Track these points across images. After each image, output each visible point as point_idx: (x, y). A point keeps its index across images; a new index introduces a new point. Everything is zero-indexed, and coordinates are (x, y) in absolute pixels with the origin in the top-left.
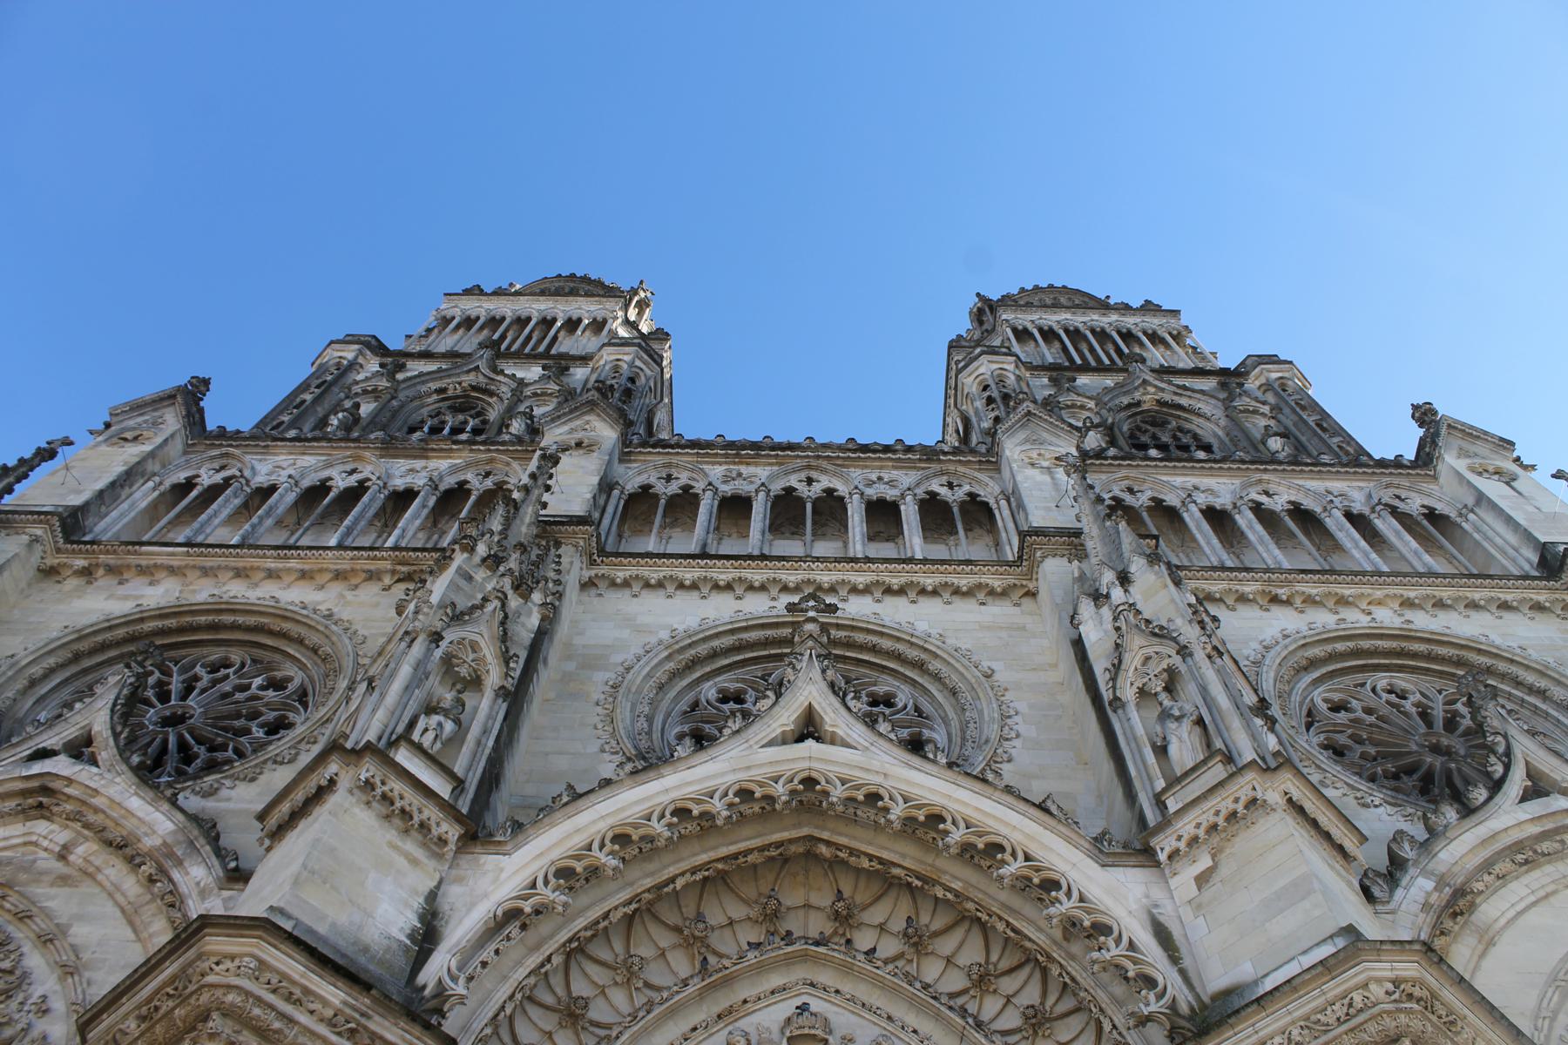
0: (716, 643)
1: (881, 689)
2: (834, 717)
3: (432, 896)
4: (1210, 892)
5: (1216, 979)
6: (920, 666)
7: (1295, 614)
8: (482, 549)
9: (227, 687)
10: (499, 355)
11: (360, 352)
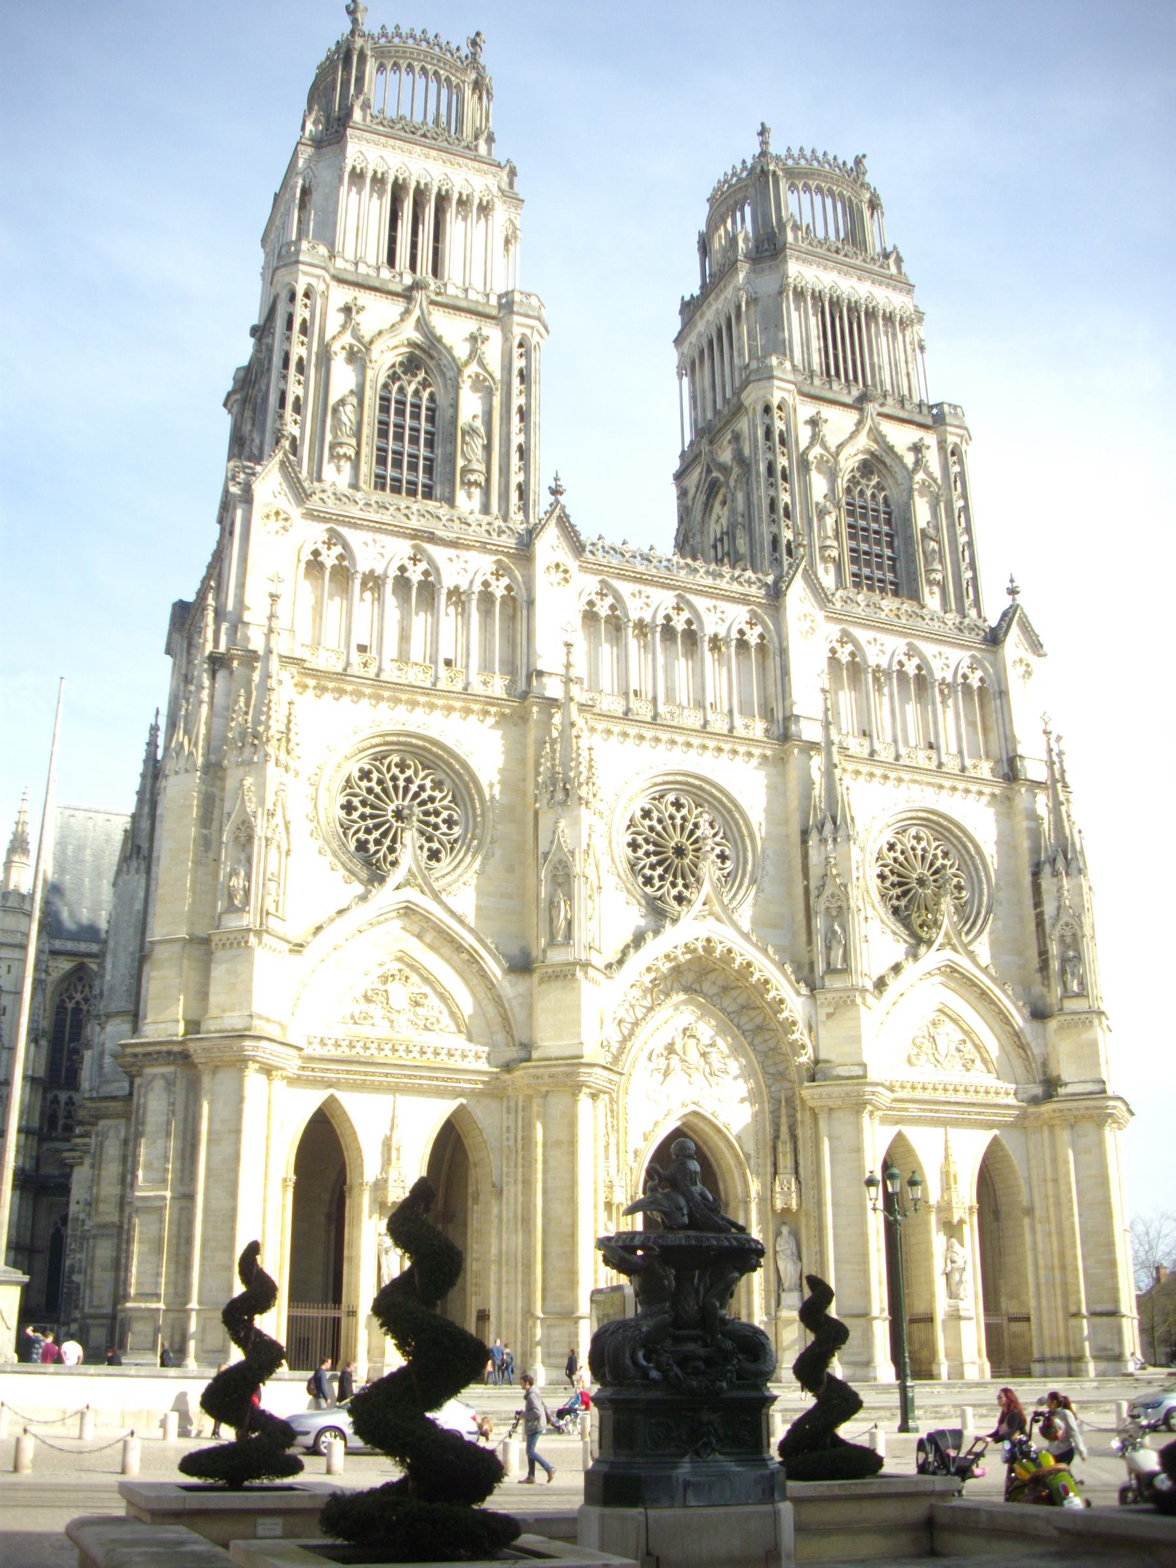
9: (414, 788)
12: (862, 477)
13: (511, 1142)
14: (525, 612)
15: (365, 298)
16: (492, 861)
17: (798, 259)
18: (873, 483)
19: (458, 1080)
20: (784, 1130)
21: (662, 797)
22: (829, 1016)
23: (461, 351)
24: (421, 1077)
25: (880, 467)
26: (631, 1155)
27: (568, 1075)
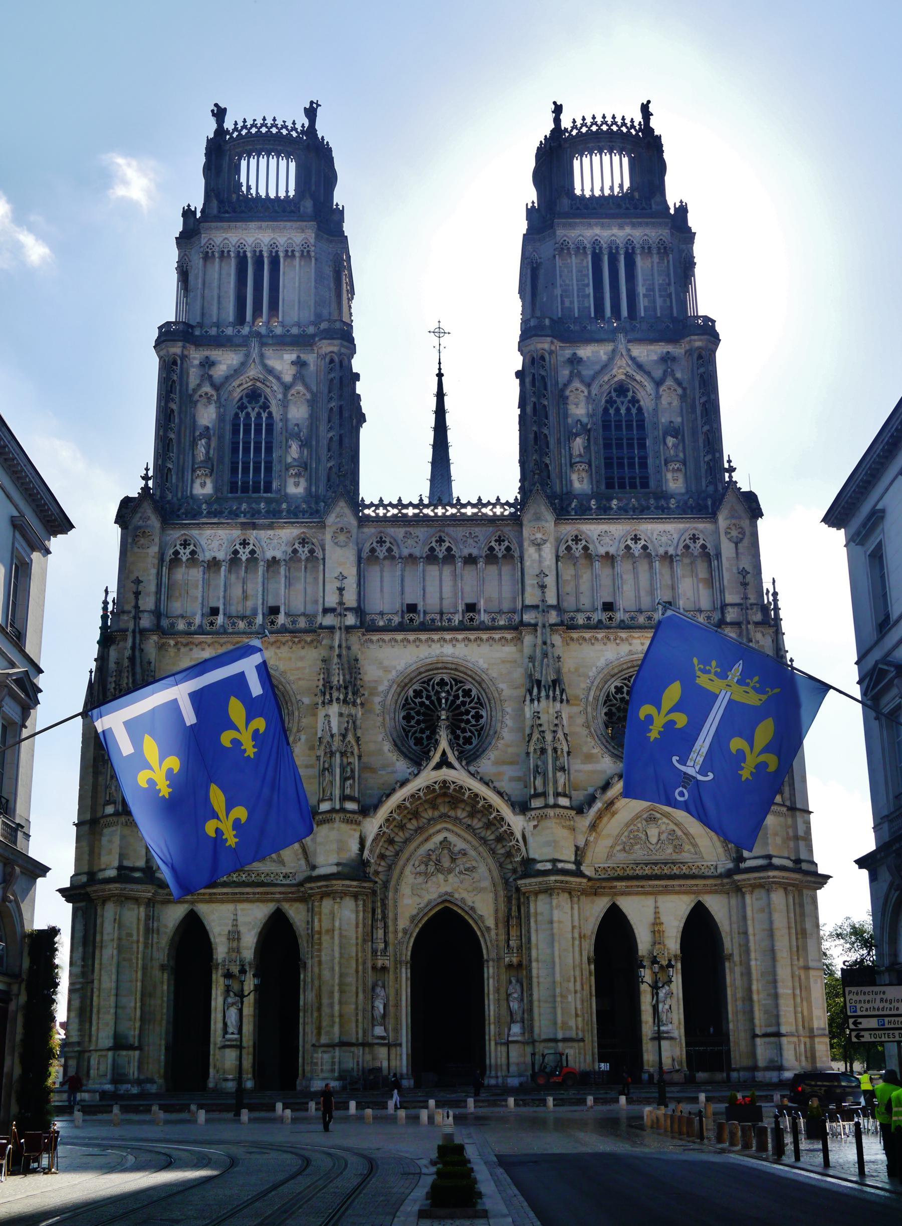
0: (412, 675)
1: (467, 687)
2: (452, 758)
3: (361, 837)
4: (535, 831)
5: (532, 856)
6: (480, 684)
7: (615, 645)
8: (342, 697)
10: (263, 344)
11: (184, 347)
12: (618, 396)
13: (310, 931)
14: (322, 566)
15: (215, 354)
16: (299, 744)
17: (565, 225)
18: (629, 398)
19: (272, 893)
20: (514, 908)
21: (430, 680)
22: (535, 827)
23: (288, 378)
24: (248, 893)
25: (634, 384)
26: (400, 935)
27: (327, 886)
